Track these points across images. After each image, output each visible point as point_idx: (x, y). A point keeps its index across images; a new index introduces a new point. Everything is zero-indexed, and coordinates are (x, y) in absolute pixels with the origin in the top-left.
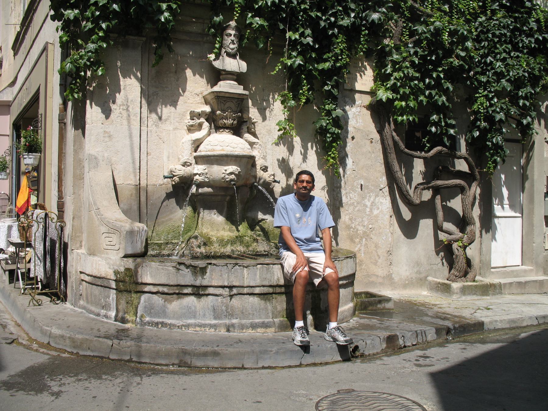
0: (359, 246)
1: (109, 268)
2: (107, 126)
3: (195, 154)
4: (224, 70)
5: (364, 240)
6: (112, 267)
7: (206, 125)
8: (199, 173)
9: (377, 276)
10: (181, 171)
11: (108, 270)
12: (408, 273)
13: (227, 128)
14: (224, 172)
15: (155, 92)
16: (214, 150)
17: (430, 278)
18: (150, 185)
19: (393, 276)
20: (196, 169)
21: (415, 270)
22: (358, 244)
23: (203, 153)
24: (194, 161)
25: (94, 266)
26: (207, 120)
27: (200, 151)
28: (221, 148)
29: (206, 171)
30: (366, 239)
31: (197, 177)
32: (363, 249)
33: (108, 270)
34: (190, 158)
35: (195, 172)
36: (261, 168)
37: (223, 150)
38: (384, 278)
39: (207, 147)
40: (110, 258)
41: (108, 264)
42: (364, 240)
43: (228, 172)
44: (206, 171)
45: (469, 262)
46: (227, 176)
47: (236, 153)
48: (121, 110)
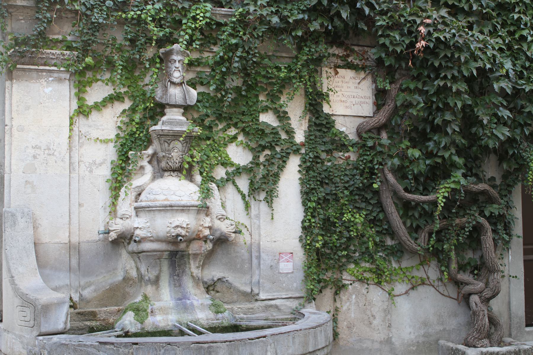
0: (348, 304)
1: (23, 348)
2: (29, 175)
3: (136, 204)
4: (168, 104)
5: (354, 297)
6: (26, 347)
7: (149, 169)
8: (140, 227)
9: (373, 341)
10: (118, 226)
11: (22, 350)
12: (413, 336)
13: (174, 171)
14: (169, 225)
15: (88, 132)
16: (157, 201)
17: (442, 342)
18: (83, 242)
19: (393, 340)
20: (137, 222)
21: (422, 332)
22: (346, 303)
23: (143, 204)
24: (134, 213)
25: (9, 344)
26: (150, 162)
27: (141, 201)
28: (164, 197)
29: (148, 224)
30: (357, 297)
31: (137, 232)
32: (353, 308)
33: (22, 350)
34: (130, 210)
35: (136, 226)
36: (217, 217)
37: (166, 200)
38: (381, 342)
39: (148, 195)
40: (24, 336)
41: (22, 342)
42: (354, 297)
43: (173, 225)
44: (148, 224)
45: (492, 321)
46: (173, 230)
47: (183, 203)
48: (46, 155)
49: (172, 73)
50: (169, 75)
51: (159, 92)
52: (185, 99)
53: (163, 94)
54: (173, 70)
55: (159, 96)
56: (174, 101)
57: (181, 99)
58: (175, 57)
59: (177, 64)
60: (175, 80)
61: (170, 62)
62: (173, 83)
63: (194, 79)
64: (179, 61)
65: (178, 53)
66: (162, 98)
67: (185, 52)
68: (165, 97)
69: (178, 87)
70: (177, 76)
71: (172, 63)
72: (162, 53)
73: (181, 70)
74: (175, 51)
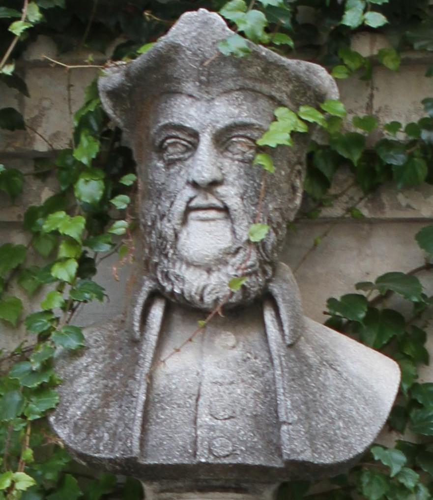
49: (167, 227)
50: (153, 251)
51: (81, 385)
52: (268, 423)
53: (107, 396)
54: (180, 206)
55: (75, 411)
56: (182, 438)
57: (241, 427)
58: (198, 111)
59: (205, 163)
60: (192, 282)
61: (161, 149)
62: (182, 309)
63: (410, 278)
64: (223, 139)
65: (216, 73)
66: (93, 420)
67: (269, 66)
68: (113, 412)
69: (227, 338)
70: (207, 248)
71: (173, 153)
72: (115, 94)
73: (234, 202)
74: (186, 63)
